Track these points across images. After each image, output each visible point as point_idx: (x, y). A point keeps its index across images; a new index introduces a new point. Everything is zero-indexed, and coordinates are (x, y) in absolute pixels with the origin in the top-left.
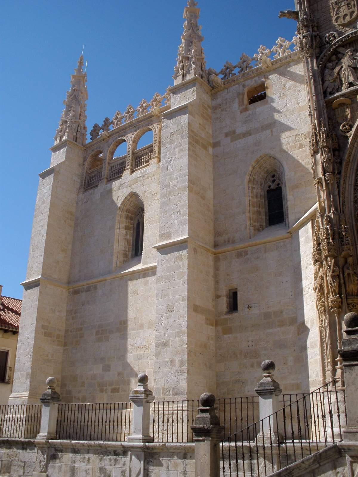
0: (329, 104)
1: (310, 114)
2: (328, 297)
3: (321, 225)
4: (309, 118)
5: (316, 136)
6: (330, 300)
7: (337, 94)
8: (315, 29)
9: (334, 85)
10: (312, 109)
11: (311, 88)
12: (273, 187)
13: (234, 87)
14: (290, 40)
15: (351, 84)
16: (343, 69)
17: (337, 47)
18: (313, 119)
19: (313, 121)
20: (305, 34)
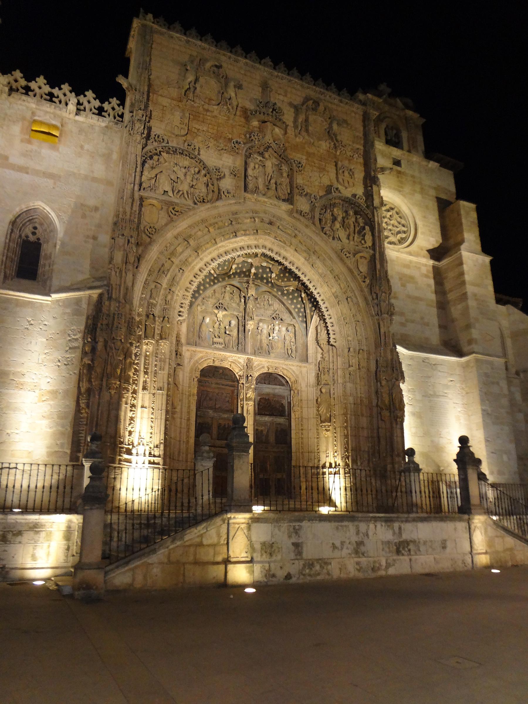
12: (32, 238)
13: (20, 107)
14: (102, 102)
15: (165, 192)
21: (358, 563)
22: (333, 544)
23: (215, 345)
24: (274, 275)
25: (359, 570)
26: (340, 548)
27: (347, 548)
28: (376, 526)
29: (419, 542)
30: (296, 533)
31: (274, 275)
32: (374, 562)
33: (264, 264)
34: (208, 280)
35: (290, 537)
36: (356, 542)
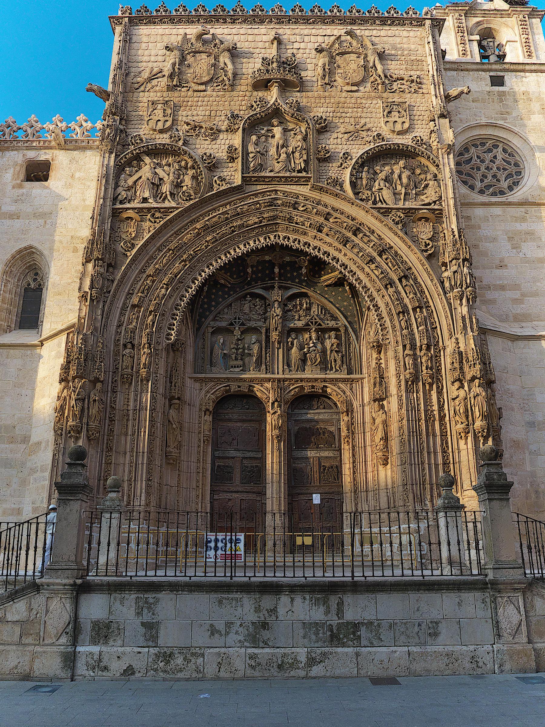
0: (116, 213)
1: (92, 218)
2: (68, 421)
3: (75, 343)
4: (90, 221)
5: (93, 244)
6: (69, 424)
7: (128, 205)
8: (123, 123)
9: (127, 195)
10: (96, 212)
11: (100, 189)
15: (145, 200)
16: (141, 180)
17: (141, 153)
18: (94, 224)
19: (94, 226)
20: (110, 123)
21: (252, 657)
22: (212, 625)
23: (231, 370)
24: (304, 271)
25: (253, 667)
26: (223, 632)
27: (237, 633)
28: (292, 600)
29: (379, 625)
30: (149, 608)
31: (304, 271)
32: (284, 655)
33: (288, 259)
34: (220, 293)
35: (139, 614)
36: (253, 623)
